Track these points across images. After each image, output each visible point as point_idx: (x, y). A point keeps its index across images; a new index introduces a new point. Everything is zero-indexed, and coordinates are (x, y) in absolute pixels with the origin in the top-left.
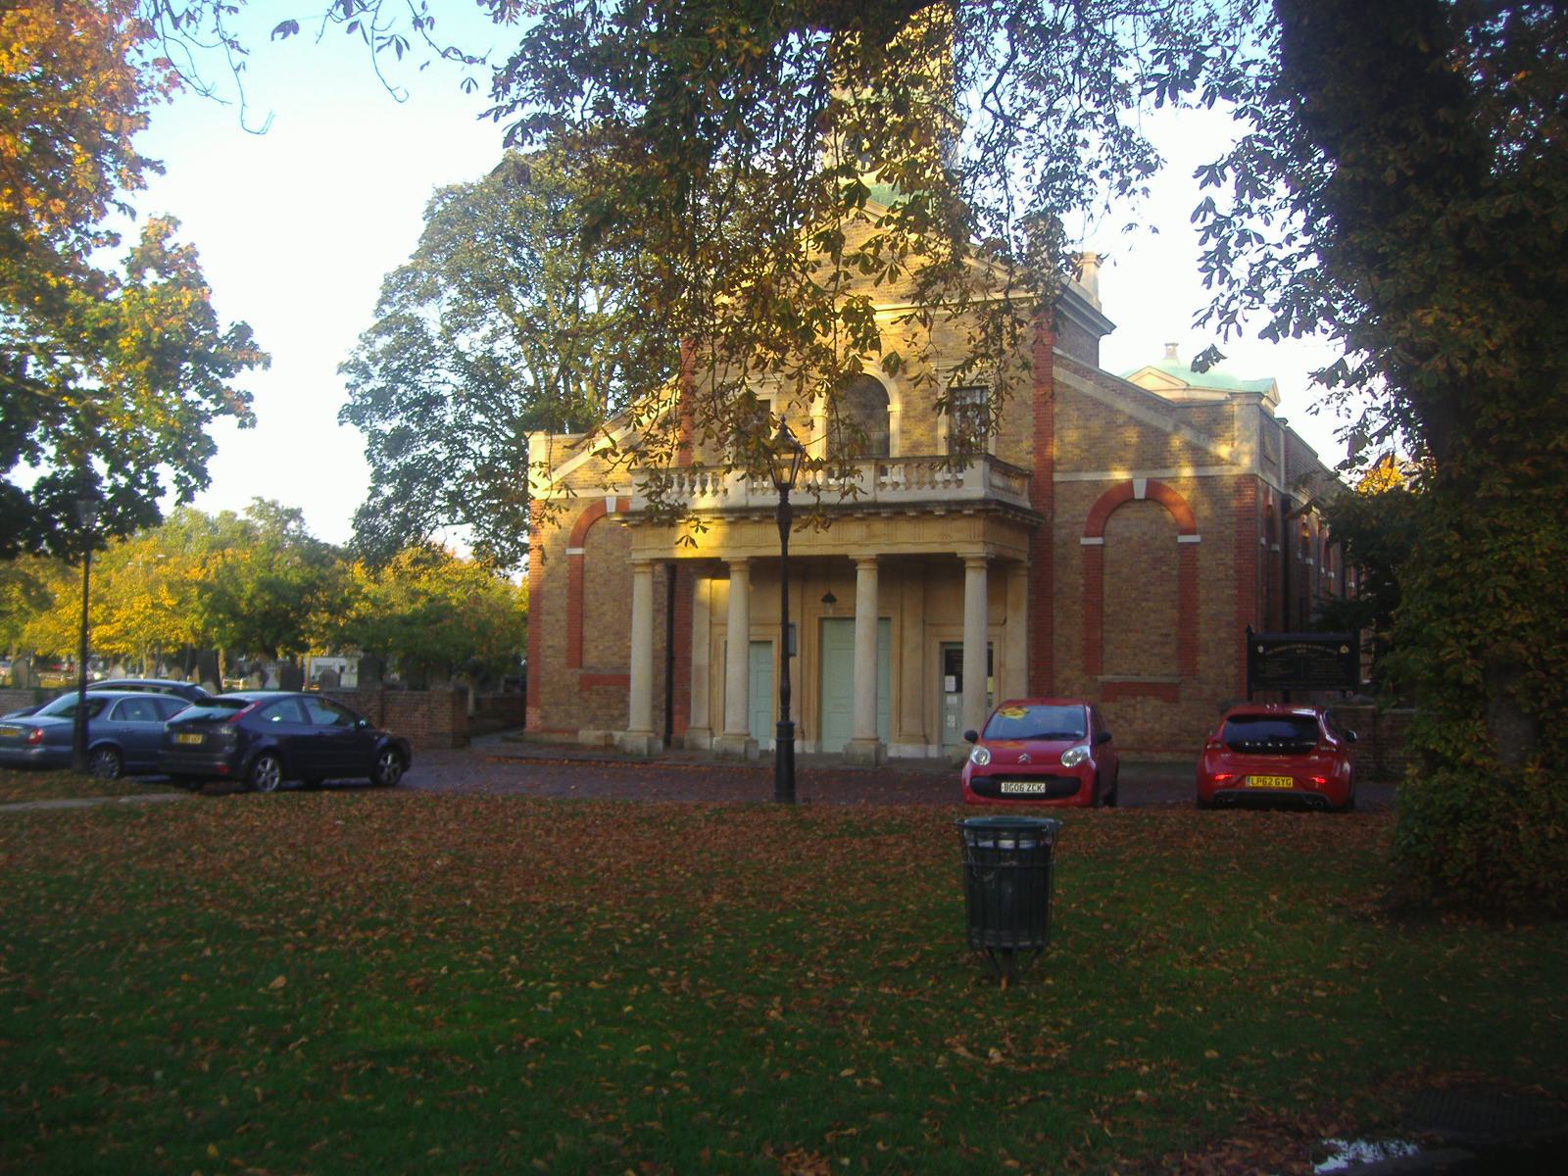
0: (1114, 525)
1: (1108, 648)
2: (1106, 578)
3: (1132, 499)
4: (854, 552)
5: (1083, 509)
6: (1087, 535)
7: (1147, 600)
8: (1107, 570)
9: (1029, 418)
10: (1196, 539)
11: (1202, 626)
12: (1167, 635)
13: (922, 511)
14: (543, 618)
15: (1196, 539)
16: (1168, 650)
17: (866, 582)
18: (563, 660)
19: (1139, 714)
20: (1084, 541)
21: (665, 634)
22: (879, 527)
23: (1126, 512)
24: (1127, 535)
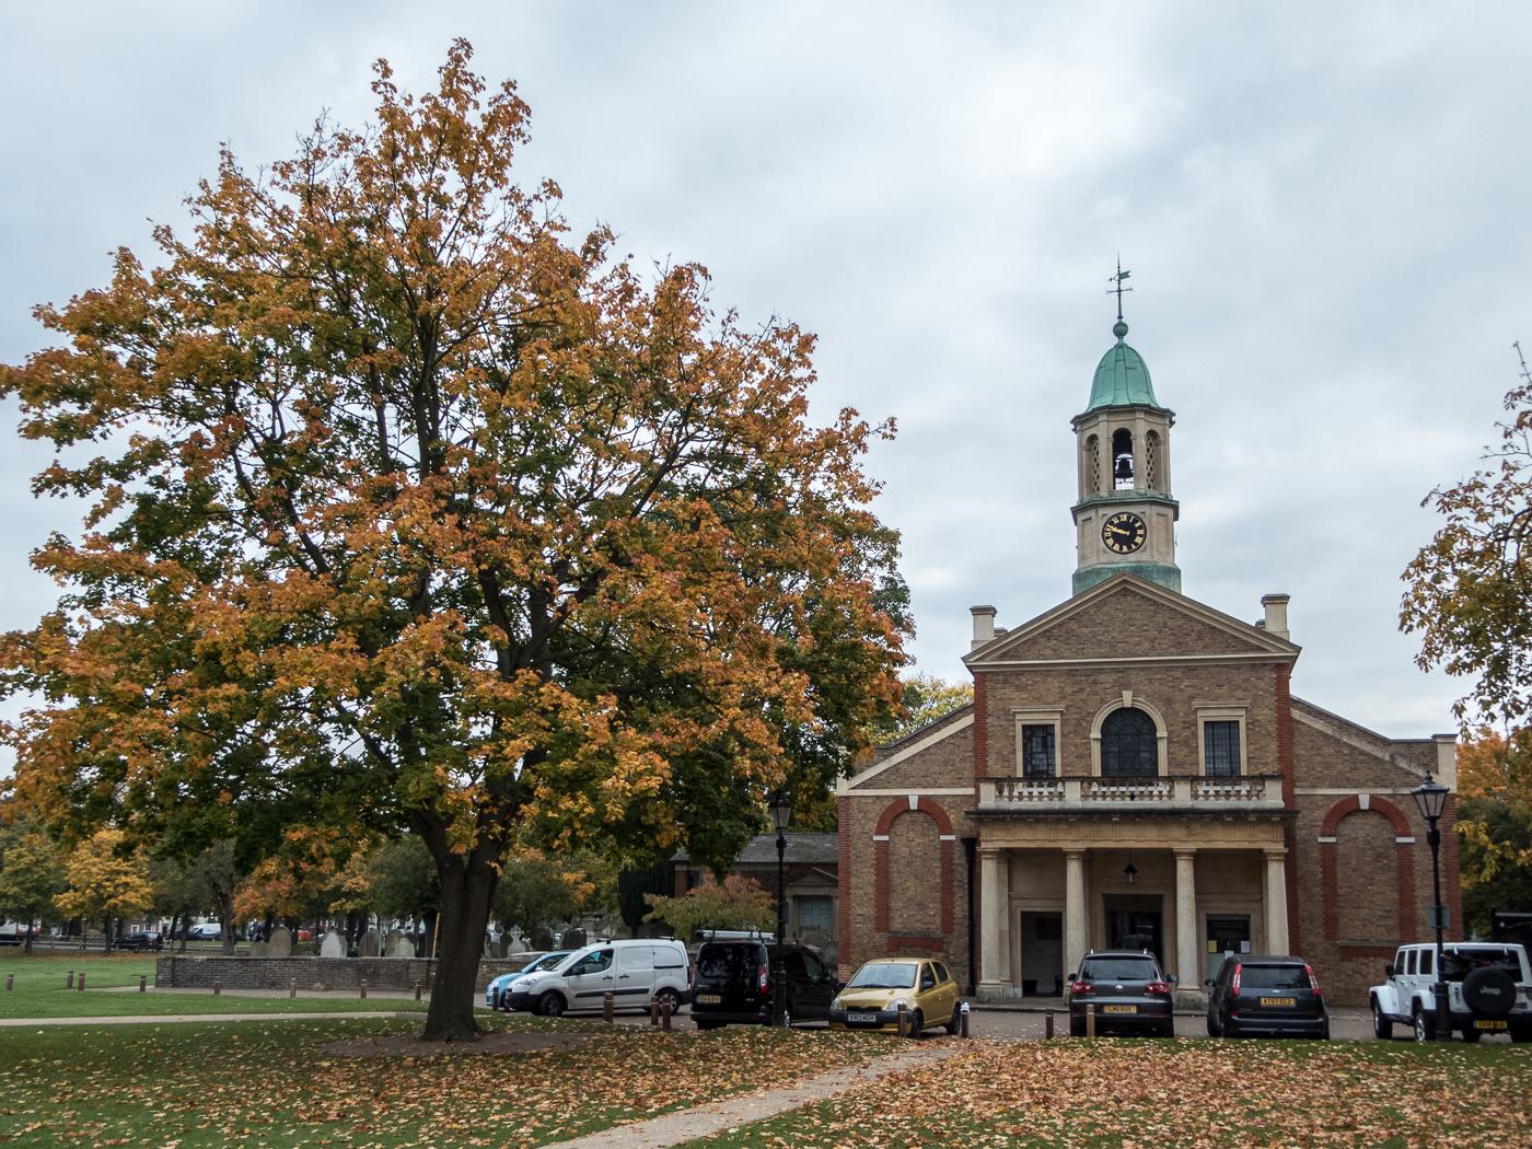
0: (1345, 829)
1: (1343, 921)
2: (1338, 867)
3: (1359, 810)
4: (1176, 846)
5: (1320, 814)
6: (1323, 835)
7: (1371, 885)
8: (1340, 862)
9: (1274, 746)
10: (1412, 840)
11: (1419, 905)
12: (1389, 911)
13: (1238, 817)
14: (852, 891)
15: (1412, 840)
16: (1390, 922)
17: (1184, 870)
18: (871, 926)
19: (1371, 970)
20: (1320, 840)
21: (966, 907)
22: (1197, 828)
23: (1355, 820)
24: (1353, 835)
